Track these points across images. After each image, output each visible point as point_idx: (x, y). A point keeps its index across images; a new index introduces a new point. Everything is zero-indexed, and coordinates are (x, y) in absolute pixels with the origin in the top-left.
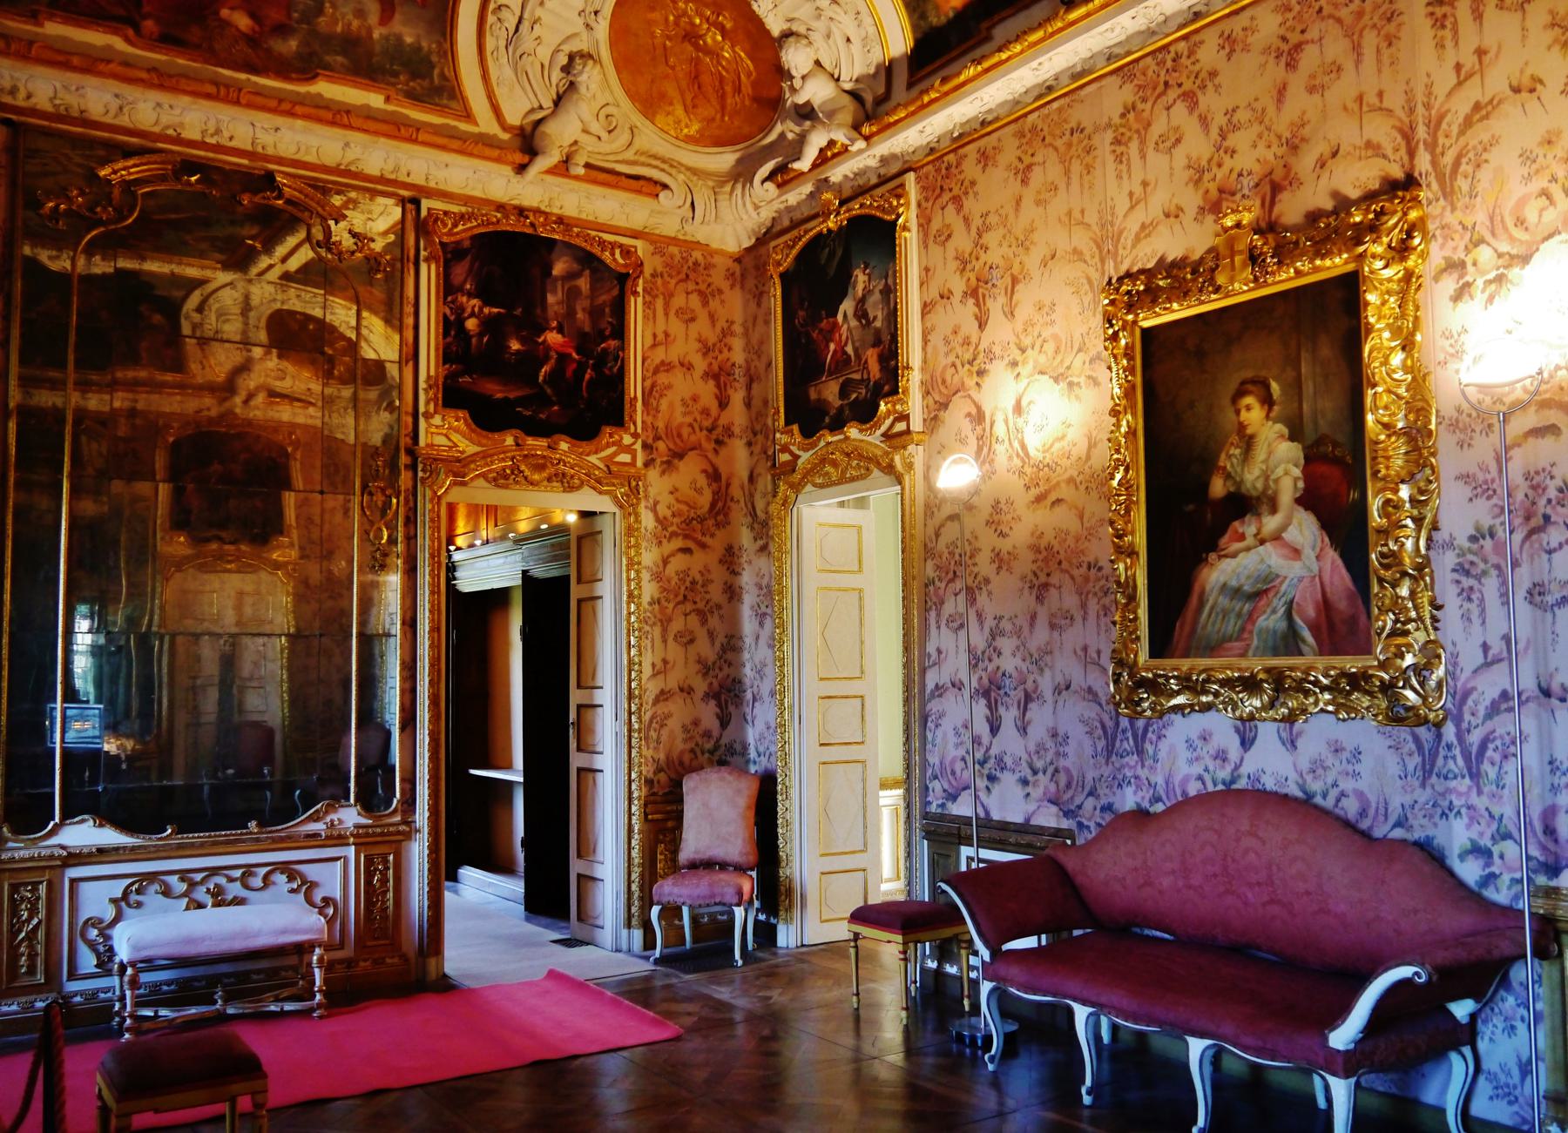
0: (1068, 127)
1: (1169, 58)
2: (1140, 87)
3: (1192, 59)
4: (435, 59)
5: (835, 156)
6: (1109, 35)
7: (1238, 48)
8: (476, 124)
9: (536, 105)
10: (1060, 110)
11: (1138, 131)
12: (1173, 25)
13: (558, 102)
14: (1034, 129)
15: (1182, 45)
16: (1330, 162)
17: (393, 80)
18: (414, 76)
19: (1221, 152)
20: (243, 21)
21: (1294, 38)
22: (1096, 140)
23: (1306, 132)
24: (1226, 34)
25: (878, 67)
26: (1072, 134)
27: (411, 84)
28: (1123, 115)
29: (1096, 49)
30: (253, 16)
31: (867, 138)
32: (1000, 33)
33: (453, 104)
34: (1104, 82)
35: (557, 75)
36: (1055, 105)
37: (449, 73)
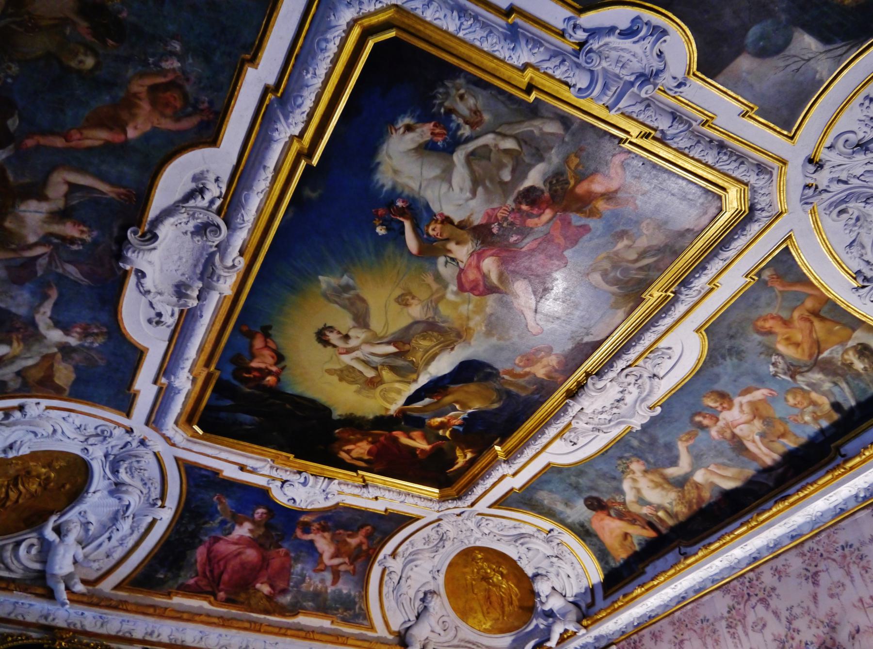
1: (746, 581)
2: (734, 596)
3: (759, 581)
4: (357, 600)
5: (569, 637)
6: (710, 570)
7: (783, 575)
8: (376, 632)
9: (407, 619)
10: (692, 609)
11: (740, 621)
12: (743, 564)
13: (418, 617)
14: (679, 620)
15: (751, 574)
16: (857, 636)
17: (336, 612)
18: (347, 609)
19: (791, 631)
20: (266, 589)
21: (813, 569)
22: (717, 626)
23: (836, 618)
24: (774, 567)
25: (586, 589)
27: (345, 613)
28: (729, 612)
29: (704, 577)
30: (271, 586)
31: (586, 627)
32: (650, 570)
33: (365, 622)
34: (713, 594)
35: (418, 603)
36: (689, 607)
37: (364, 607)
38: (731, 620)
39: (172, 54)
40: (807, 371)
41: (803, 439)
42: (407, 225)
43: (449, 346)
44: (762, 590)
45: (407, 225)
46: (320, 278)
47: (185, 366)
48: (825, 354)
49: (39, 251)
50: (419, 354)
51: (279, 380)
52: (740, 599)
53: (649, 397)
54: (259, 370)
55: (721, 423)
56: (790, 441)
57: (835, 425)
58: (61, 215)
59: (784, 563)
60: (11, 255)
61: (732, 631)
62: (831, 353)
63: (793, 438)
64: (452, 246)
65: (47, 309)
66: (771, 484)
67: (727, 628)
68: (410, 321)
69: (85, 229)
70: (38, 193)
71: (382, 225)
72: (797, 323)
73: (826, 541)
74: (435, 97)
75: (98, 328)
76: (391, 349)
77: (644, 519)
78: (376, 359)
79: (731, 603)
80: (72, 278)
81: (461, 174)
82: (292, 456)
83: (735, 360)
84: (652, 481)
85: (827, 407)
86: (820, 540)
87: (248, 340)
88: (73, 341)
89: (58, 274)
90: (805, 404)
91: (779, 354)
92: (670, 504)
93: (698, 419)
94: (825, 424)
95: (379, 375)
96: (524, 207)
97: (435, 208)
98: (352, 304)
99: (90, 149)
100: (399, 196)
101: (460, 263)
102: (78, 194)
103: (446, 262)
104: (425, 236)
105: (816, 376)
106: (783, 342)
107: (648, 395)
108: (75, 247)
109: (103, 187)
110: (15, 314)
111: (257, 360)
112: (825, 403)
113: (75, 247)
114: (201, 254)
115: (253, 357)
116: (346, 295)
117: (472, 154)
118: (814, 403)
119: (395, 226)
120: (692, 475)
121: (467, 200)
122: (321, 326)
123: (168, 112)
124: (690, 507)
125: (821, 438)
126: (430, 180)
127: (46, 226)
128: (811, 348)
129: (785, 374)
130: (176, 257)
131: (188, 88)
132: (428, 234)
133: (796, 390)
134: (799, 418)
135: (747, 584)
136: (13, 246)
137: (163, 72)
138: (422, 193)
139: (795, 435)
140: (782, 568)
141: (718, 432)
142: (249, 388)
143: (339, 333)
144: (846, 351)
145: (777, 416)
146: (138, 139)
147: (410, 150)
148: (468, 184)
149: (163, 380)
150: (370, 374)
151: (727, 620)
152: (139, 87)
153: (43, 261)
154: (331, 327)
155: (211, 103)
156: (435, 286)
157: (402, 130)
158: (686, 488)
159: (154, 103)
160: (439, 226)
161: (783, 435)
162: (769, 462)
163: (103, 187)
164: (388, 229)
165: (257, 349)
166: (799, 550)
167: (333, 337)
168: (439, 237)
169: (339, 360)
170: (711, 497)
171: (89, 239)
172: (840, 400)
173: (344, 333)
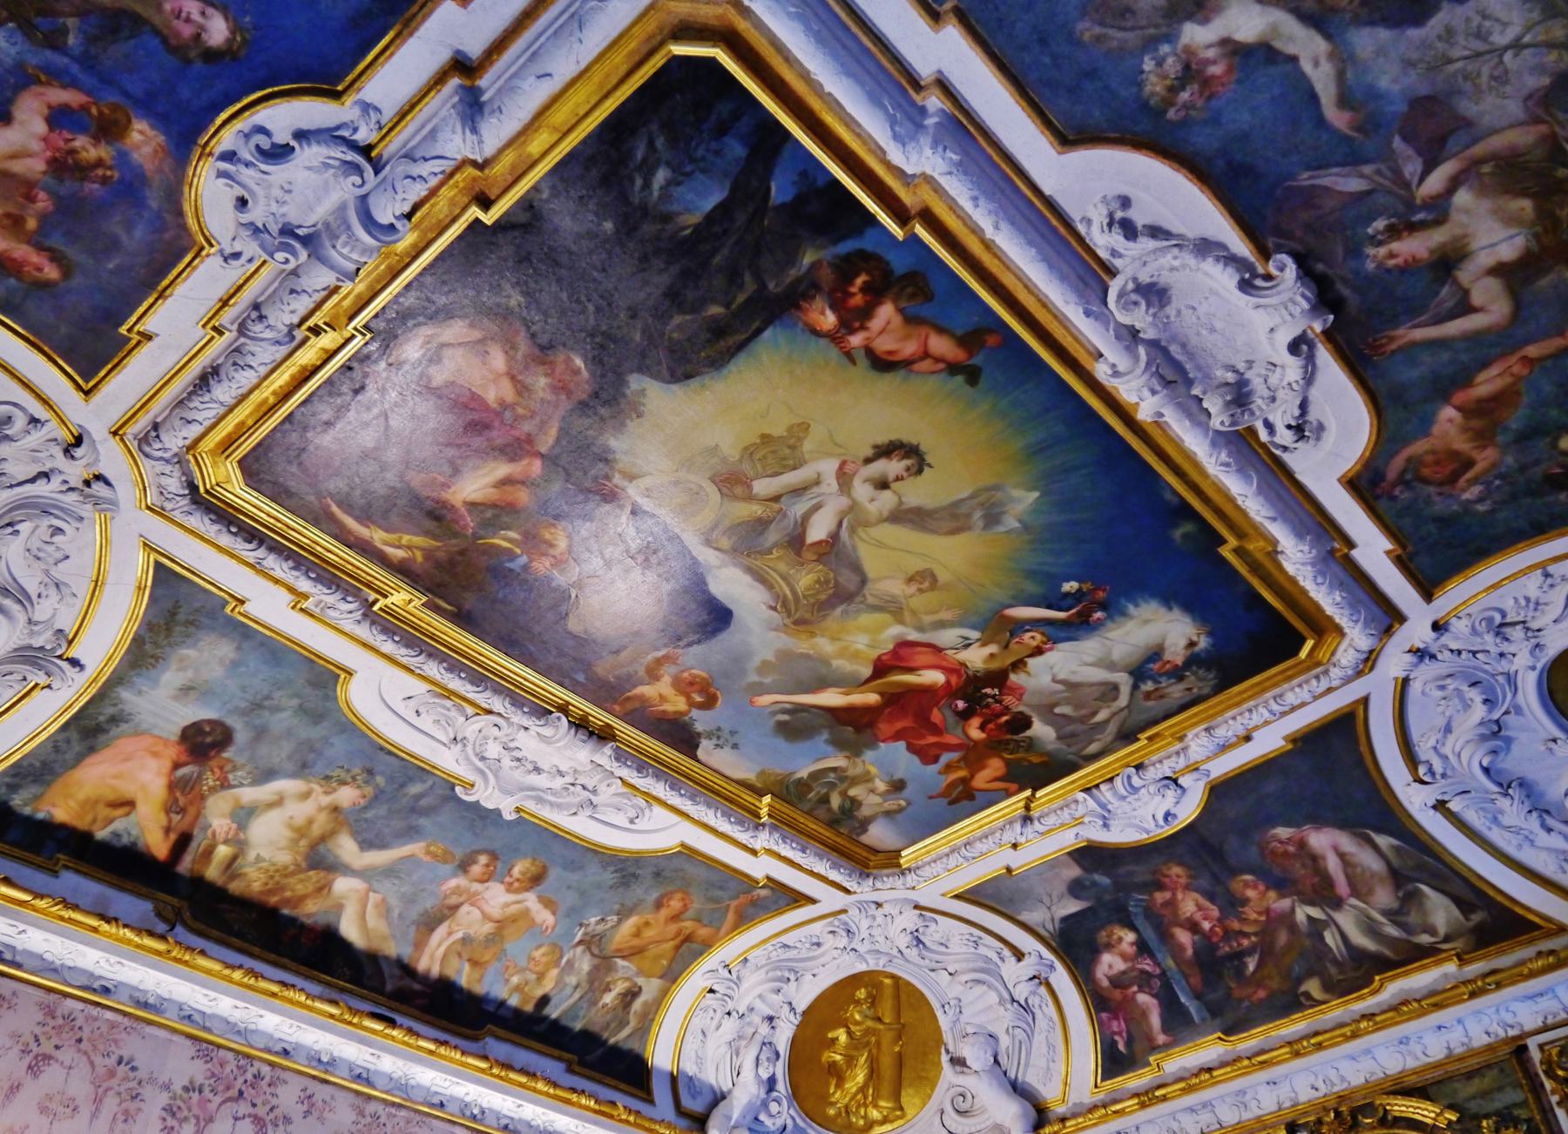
0: (119, 1052)
1: (254, 1070)
2: (213, 1075)
3: (272, 1090)
6: (205, 1001)
7: (316, 1114)
10: (113, 1025)
11: (197, 1118)
14: (69, 1018)
15: (266, 1069)
24: (309, 1092)
26: (119, 1063)
28: (186, 1089)
34: (176, 1038)
38: (179, 1103)
40: (593, 955)
41: (479, 989)
42: (1062, 615)
43: (782, 604)
44: (268, 1107)
45: (1062, 615)
46: (1036, 494)
47: (979, 209)
48: (620, 962)
49: (1435, 182)
50: (782, 567)
51: (816, 333)
52: (221, 1088)
53: (548, 807)
54: (866, 313)
55: (476, 887)
56: (469, 976)
57: (517, 1012)
58: (1447, 263)
59: (328, 1099)
60: (1479, 150)
61: (171, 1122)
62: (623, 967)
63: (476, 975)
65: (1322, 78)
66: (389, 987)
67: (164, 1109)
68: (871, 574)
69: (1391, 262)
70: (1511, 274)
72: (673, 928)
73: (402, 1124)
75: (1187, 106)
76: (818, 531)
77: (193, 824)
78: (799, 508)
79: (199, 1079)
80: (1334, 170)
82: (489, 218)
83: (611, 882)
84: (310, 822)
85: (539, 993)
86: (395, 1116)
87: (959, 332)
88: (1198, 35)
89: (1367, 161)
90: (537, 969)
91: (620, 921)
92: (259, 859)
93: (483, 859)
94: (514, 1001)
95: (750, 498)
96: (1005, 718)
98: (955, 517)
99: (1485, 364)
102: (1450, 304)
103: (967, 639)
105: (585, 964)
106: (644, 920)
107: (552, 804)
108: (1380, 224)
110: (1372, 23)
111: (897, 320)
112: (547, 986)
113: (1380, 224)
114: (1199, 368)
115: (911, 320)
116: (978, 515)
118: (541, 976)
119: (1070, 601)
120: (345, 875)
122: (929, 459)
123: (1429, 458)
124: (271, 892)
125: (491, 1008)
127: (1458, 231)
128: (632, 947)
129: (586, 934)
130: (1218, 325)
132: (1028, 631)
133: (557, 950)
134: (511, 971)
135: (249, 1076)
136: (1486, 169)
138: (1097, 638)
139: (482, 977)
140: (320, 1103)
141: (458, 887)
142: (815, 266)
143: (898, 479)
144: (627, 979)
145: (508, 946)
146: (1434, 414)
147: (1164, 640)
149: (934, 102)
150: (763, 487)
151: (174, 1098)
153: (1412, 168)
154: (920, 471)
155: (1393, 498)
156: (927, 619)
158: (311, 873)
159: (1455, 454)
161: (475, 963)
162: (422, 965)
164: (1067, 594)
165: (927, 337)
166: (359, 1101)
167: (893, 467)
169: (829, 455)
170: (309, 915)
171: (1371, 251)
172: (552, 1003)
173: (894, 486)
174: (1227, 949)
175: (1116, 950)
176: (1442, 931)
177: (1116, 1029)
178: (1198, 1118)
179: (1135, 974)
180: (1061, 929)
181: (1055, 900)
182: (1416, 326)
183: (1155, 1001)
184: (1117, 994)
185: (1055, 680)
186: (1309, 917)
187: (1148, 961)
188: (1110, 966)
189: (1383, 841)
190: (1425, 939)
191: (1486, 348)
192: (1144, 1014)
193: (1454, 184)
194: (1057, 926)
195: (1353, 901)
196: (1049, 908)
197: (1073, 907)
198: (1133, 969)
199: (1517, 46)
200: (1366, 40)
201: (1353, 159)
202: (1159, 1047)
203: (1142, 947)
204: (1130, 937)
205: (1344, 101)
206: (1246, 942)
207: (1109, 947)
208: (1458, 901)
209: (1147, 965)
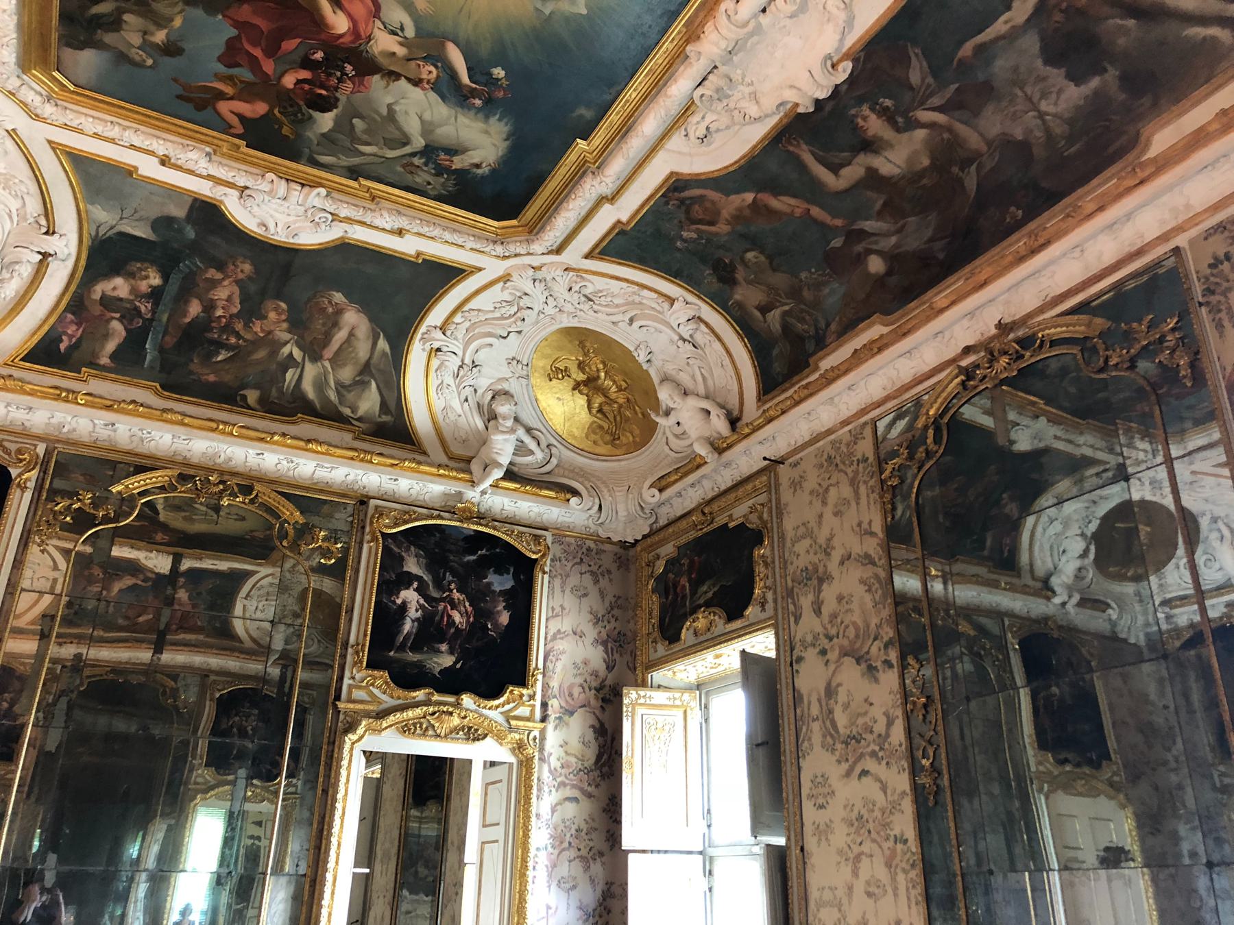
39: (685, 241)
42: (465, 79)
45: (465, 79)
46: (584, 12)
49: (925, 116)
58: (869, 145)
64: (401, 51)
69: (859, 120)
70: (873, 179)
71: (498, 80)
74: (455, 185)
80: (925, 64)
81: (412, 126)
89: (935, 76)
97: (433, 96)
99: (795, 196)
100: (479, 110)
101: (382, 27)
103: (402, 29)
104: (439, 65)
108: (888, 102)
109: (808, 158)
110: (1042, 40)
113: (888, 102)
117: (405, 144)
119: (483, 79)
121: (396, 103)
123: (708, 205)
126: (446, 124)
131: (683, 217)
132: (436, 67)
136: (946, 136)
137: (698, 231)
146: (749, 191)
148: (401, 118)
152: (722, 228)
153: (936, 101)
157: (484, 165)
159: (718, 213)
160: (424, 76)
163: (808, 158)
168: (421, 63)
174: (216, 336)
175: (133, 282)
176: (360, 413)
177: (69, 332)
178: (112, 433)
179: (128, 306)
180: (110, 238)
181: (137, 216)
182: (813, 154)
183: (124, 333)
184: (97, 310)
185: (389, 106)
186: (291, 354)
187: (149, 306)
188: (114, 289)
189: (383, 344)
190: (347, 411)
191: (813, 191)
192: (106, 336)
193: (931, 126)
194: (110, 233)
195: (327, 364)
196: (121, 219)
197: (141, 231)
198: (131, 302)
199: (1041, 115)
200: (1031, 43)
201: (935, 71)
202: (99, 365)
203: (155, 295)
204: (156, 280)
205: (981, 49)
206: (233, 340)
207: (131, 275)
208: (384, 406)
209: (145, 308)
